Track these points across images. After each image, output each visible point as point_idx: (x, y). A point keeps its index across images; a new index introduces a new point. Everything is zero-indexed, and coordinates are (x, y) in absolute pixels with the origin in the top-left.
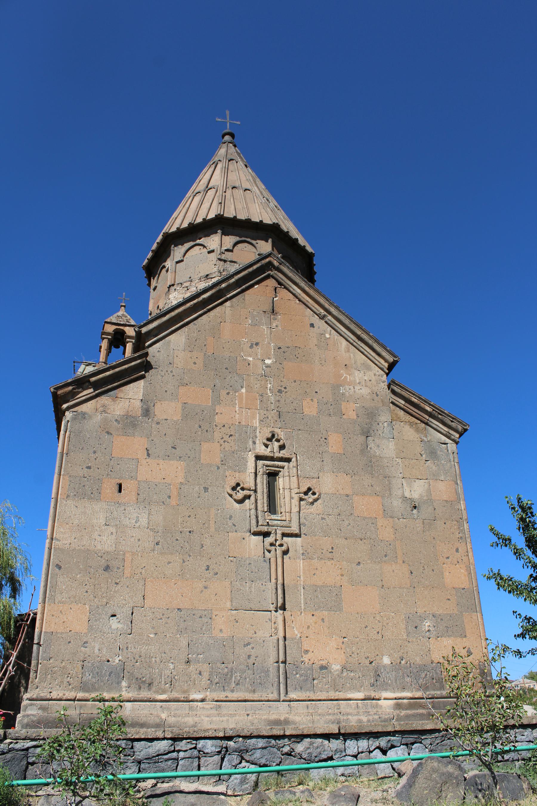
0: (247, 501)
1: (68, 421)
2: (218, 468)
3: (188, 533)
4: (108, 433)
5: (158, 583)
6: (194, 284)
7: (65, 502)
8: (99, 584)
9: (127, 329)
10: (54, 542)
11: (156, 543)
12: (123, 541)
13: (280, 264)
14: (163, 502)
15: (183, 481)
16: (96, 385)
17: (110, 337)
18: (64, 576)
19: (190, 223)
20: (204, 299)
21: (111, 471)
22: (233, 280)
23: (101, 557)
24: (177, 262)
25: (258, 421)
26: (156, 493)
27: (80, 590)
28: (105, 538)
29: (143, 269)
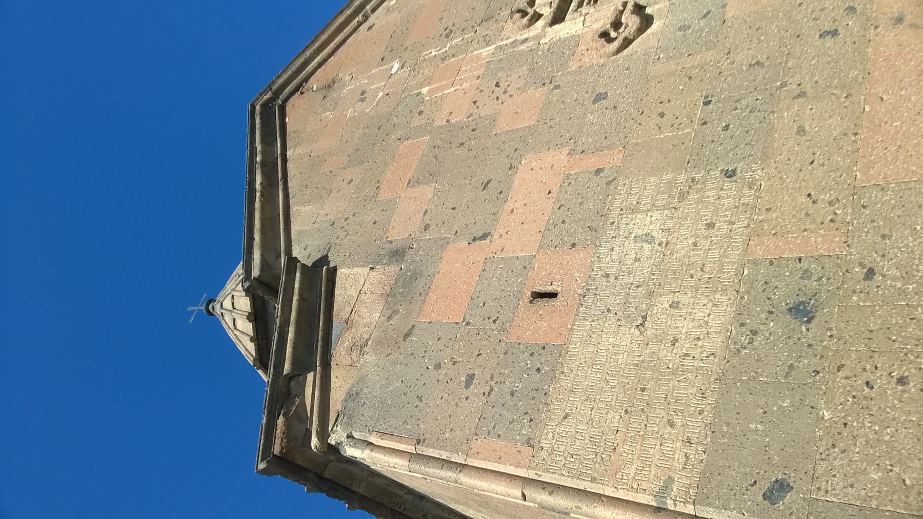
0: (649, 11)
1: (350, 437)
2: (557, 87)
3: (711, 106)
4: (407, 335)
5: (874, 149)
7: (544, 454)
8: (869, 335)
10: (670, 505)
11: (730, 177)
12: (707, 270)
13: (271, 89)
14: (608, 183)
15: (566, 150)
16: (302, 366)
18: (820, 471)
19: (247, 319)
20: (261, 183)
21: (494, 322)
22: (259, 147)
23: (754, 333)
25: (485, 49)
26: (581, 204)
27: (893, 408)
28: (685, 326)
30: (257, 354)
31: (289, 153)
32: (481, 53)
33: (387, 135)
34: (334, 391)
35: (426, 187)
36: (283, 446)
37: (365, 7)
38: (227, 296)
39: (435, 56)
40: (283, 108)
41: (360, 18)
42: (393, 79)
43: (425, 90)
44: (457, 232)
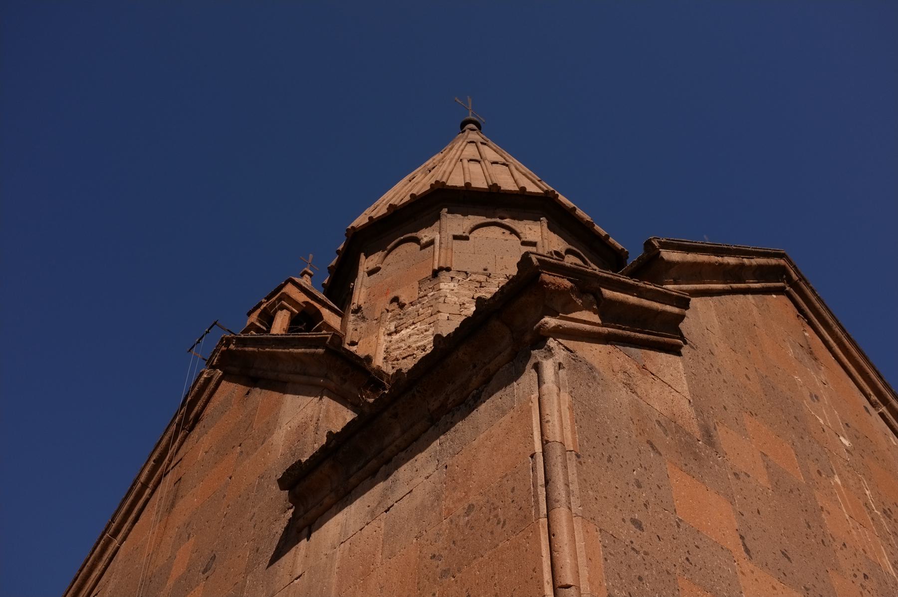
6: (497, 282)
9: (325, 312)
17: (296, 311)
20: (728, 264)
24: (456, 237)
29: (346, 235)
30: (459, 189)
31: (750, 297)
32: (884, 557)
33: (793, 428)
34: (589, 348)
35: (766, 477)
36: (550, 285)
37: (884, 405)
38: (505, 158)
39: (866, 495)
40: (779, 291)
41: (874, 398)
42: (837, 438)
43: (837, 479)
44: (743, 515)
